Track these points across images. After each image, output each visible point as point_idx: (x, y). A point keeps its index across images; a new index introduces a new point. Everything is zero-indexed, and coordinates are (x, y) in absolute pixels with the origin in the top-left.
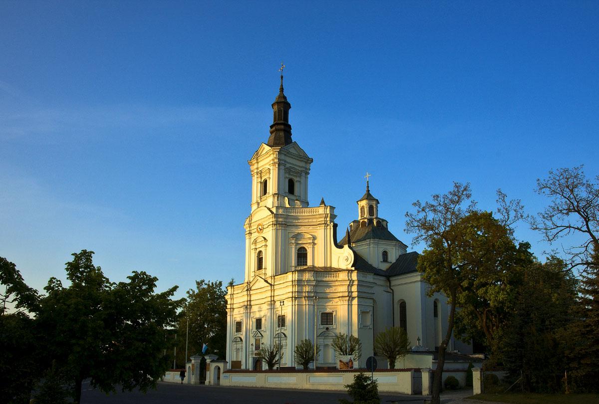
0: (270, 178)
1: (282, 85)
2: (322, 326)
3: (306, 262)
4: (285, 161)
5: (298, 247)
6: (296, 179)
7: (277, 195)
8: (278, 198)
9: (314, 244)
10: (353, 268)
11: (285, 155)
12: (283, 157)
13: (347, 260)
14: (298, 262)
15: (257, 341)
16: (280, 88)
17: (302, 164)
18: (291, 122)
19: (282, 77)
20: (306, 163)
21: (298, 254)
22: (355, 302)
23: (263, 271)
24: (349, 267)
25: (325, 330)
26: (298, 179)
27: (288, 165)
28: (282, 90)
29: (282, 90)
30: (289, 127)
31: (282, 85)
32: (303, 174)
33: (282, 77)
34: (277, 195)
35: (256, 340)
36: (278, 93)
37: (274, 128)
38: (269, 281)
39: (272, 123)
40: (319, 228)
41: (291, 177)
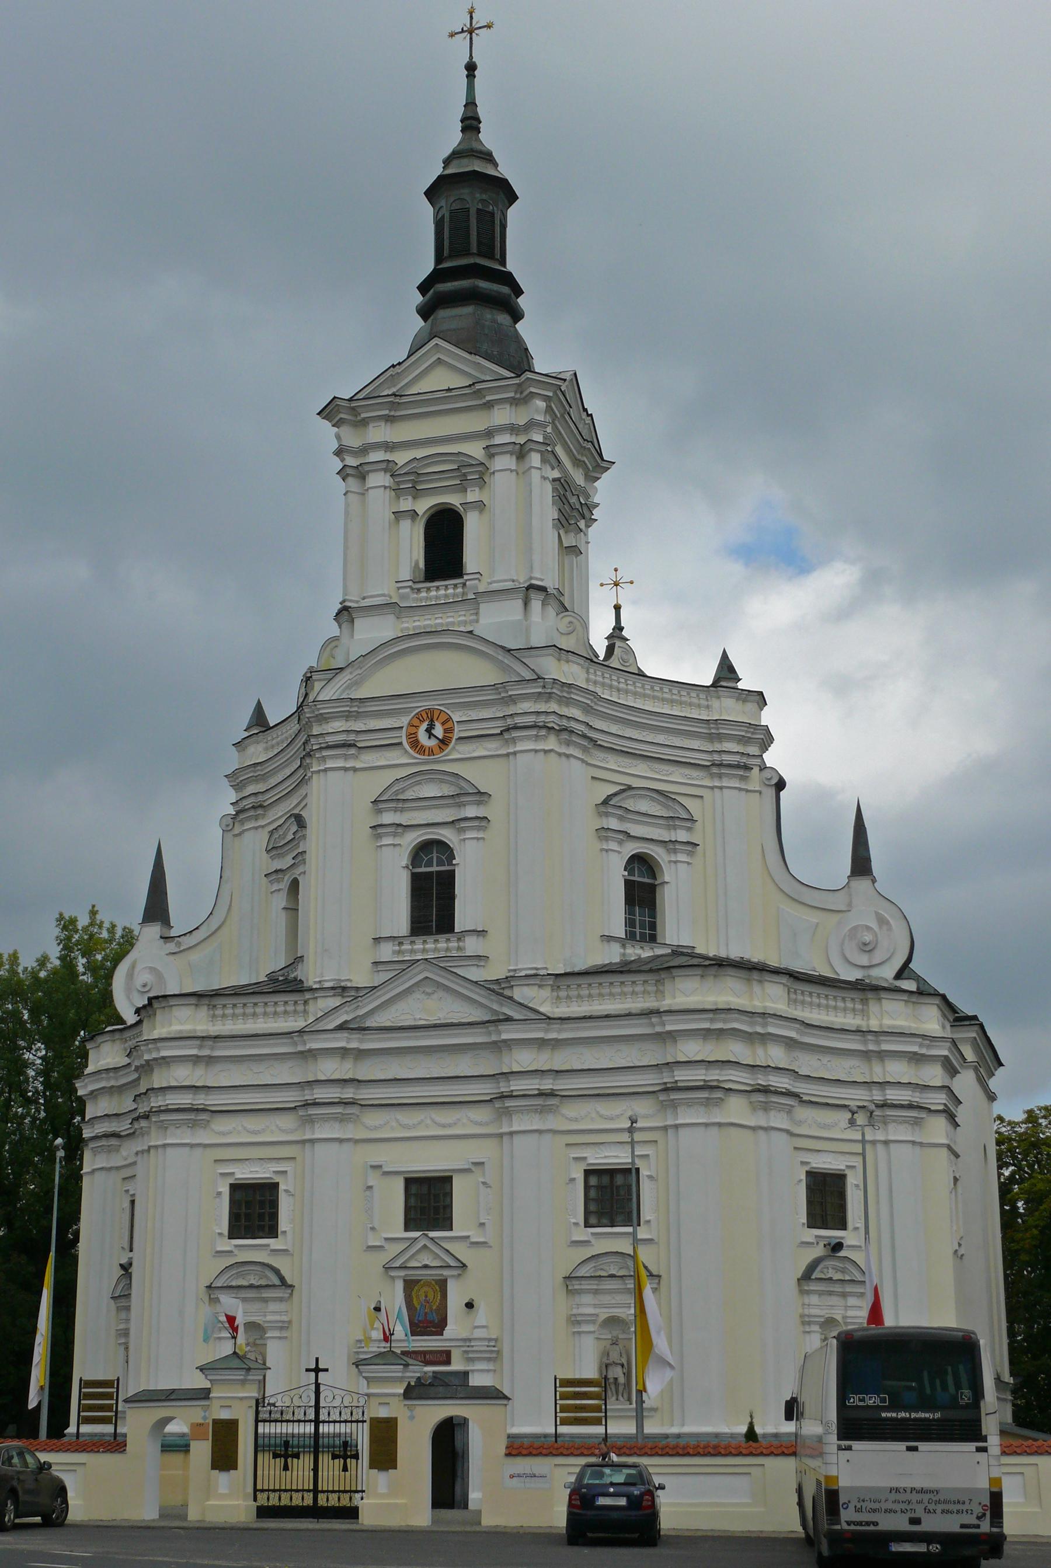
1: (471, 104)
3: (653, 926)
7: (541, 596)
14: (630, 923)
15: (419, 1295)
19: (471, 68)
21: (629, 885)
23: (472, 946)
28: (471, 123)
29: (471, 123)
31: (471, 104)
33: (471, 68)
35: (410, 1285)
38: (519, 993)
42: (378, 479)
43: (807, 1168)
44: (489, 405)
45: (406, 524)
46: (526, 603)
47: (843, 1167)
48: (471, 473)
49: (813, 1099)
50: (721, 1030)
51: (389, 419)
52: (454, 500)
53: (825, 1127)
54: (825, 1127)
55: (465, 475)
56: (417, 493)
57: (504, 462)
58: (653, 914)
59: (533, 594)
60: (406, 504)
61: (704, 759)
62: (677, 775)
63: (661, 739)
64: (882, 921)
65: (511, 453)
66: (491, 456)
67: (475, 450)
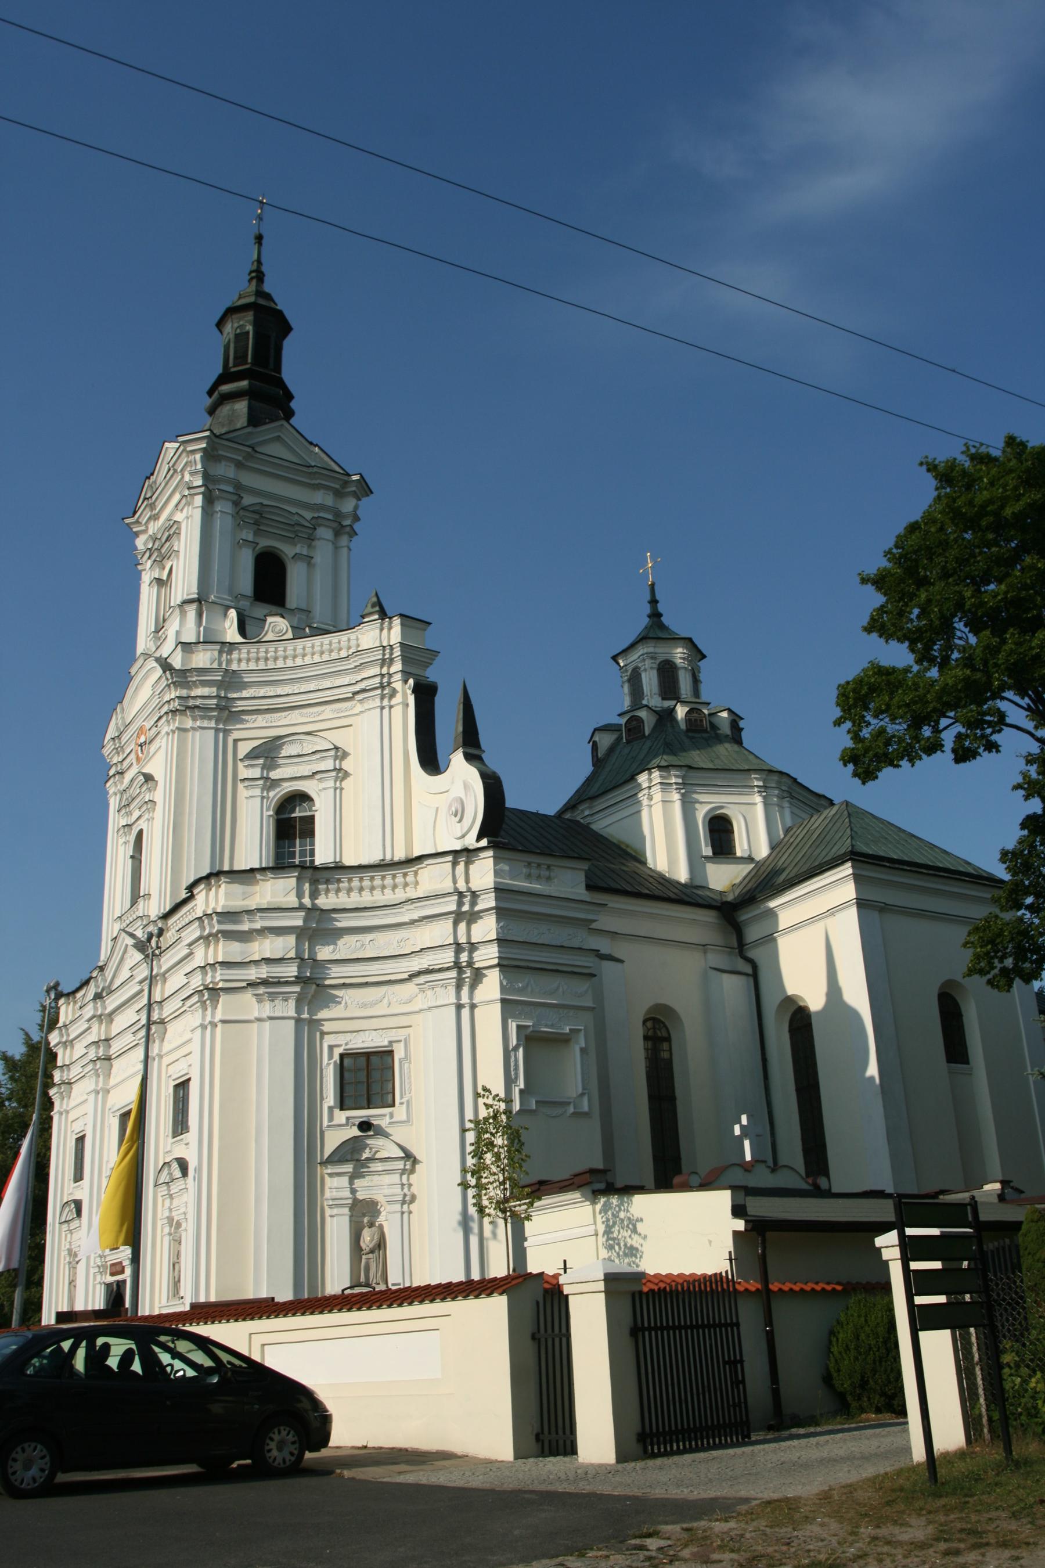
2: (341, 1116)
5: (276, 794)
6: (288, 550)
7: (194, 606)
8: (200, 615)
9: (342, 774)
10: (484, 842)
11: (239, 465)
12: (225, 470)
13: (459, 814)
17: (329, 500)
18: (289, 374)
19: (259, 239)
20: (339, 494)
22: (491, 986)
24: (471, 841)
25: (355, 1132)
26: (300, 549)
27: (248, 500)
29: (258, 276)
32: (325, 533)
33: (259, 239)
34: (194, 606)
37: (216, 395)
40: (359, 708)
41: (264, 543)
43: (341, 1050)
46: (183, 614)
47: (386, 1043)
49: (348, 981)
50: (251, 932)
53: (364, 1006)
54: (364, 1006)
58: (313, 844)
61: (347, 692)
62: (328, 711)
63: (312, 686)
64: (466, 786)
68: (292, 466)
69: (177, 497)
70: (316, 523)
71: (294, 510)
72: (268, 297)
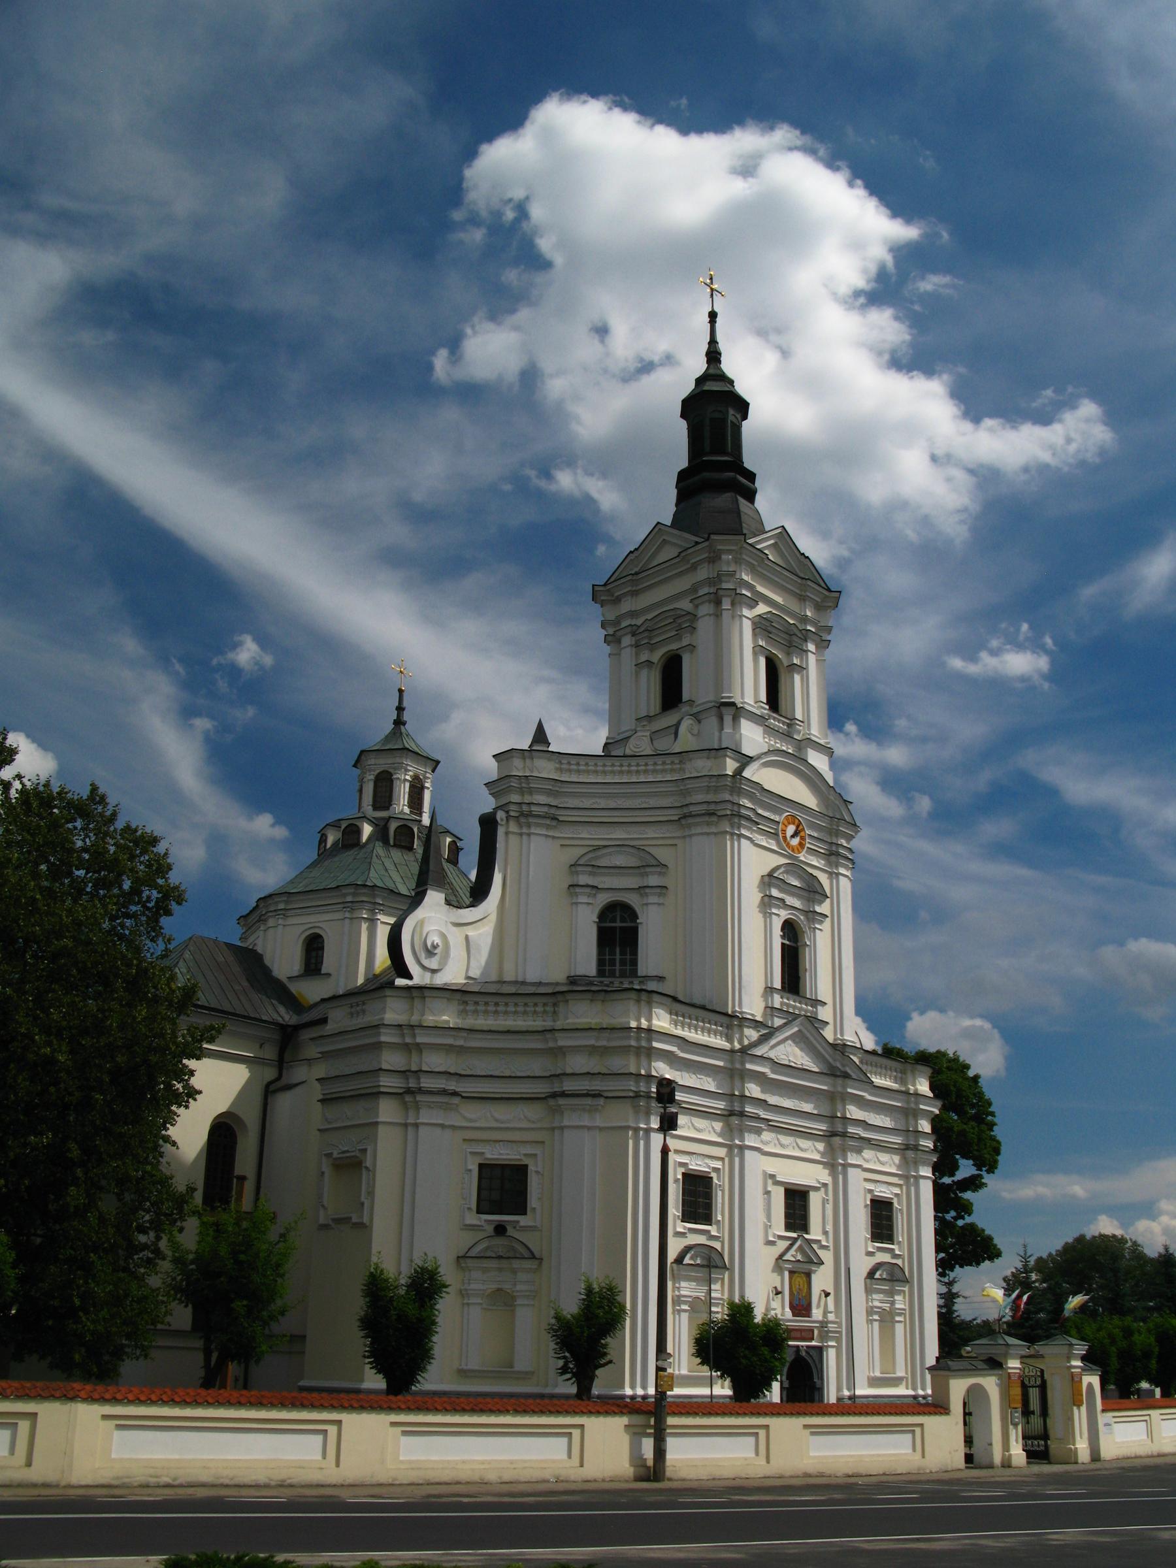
0: (692, 648)
1: (713, 342)
4: (751, 587)
7: (732, 710)
16: (705, 347)
19: (713, 316)
20: (819, 607)
27: (762, 609)
28: (713, 355)
29: (713, 355)
30: (751, 476)
31: (713, 342)
33: (713, 316)
36: (700, 366)
39: (684, 463)
42: (627, 640)
44: (694, 567)
45: (644, 673)
48: (685, 622)
51: (635, 593)
52: (674, 646)
55: (680, 624)
56: (652, 647)
57: (706, 609)
59: (724, 710)
60: (644, 657)
65: (710, 602)
66: (697, 606)
67: (685, 605)
68: (778, 569)
69: (683, 584)
70: (805, 636)
71: (792, 622)
72: (723, 378)
